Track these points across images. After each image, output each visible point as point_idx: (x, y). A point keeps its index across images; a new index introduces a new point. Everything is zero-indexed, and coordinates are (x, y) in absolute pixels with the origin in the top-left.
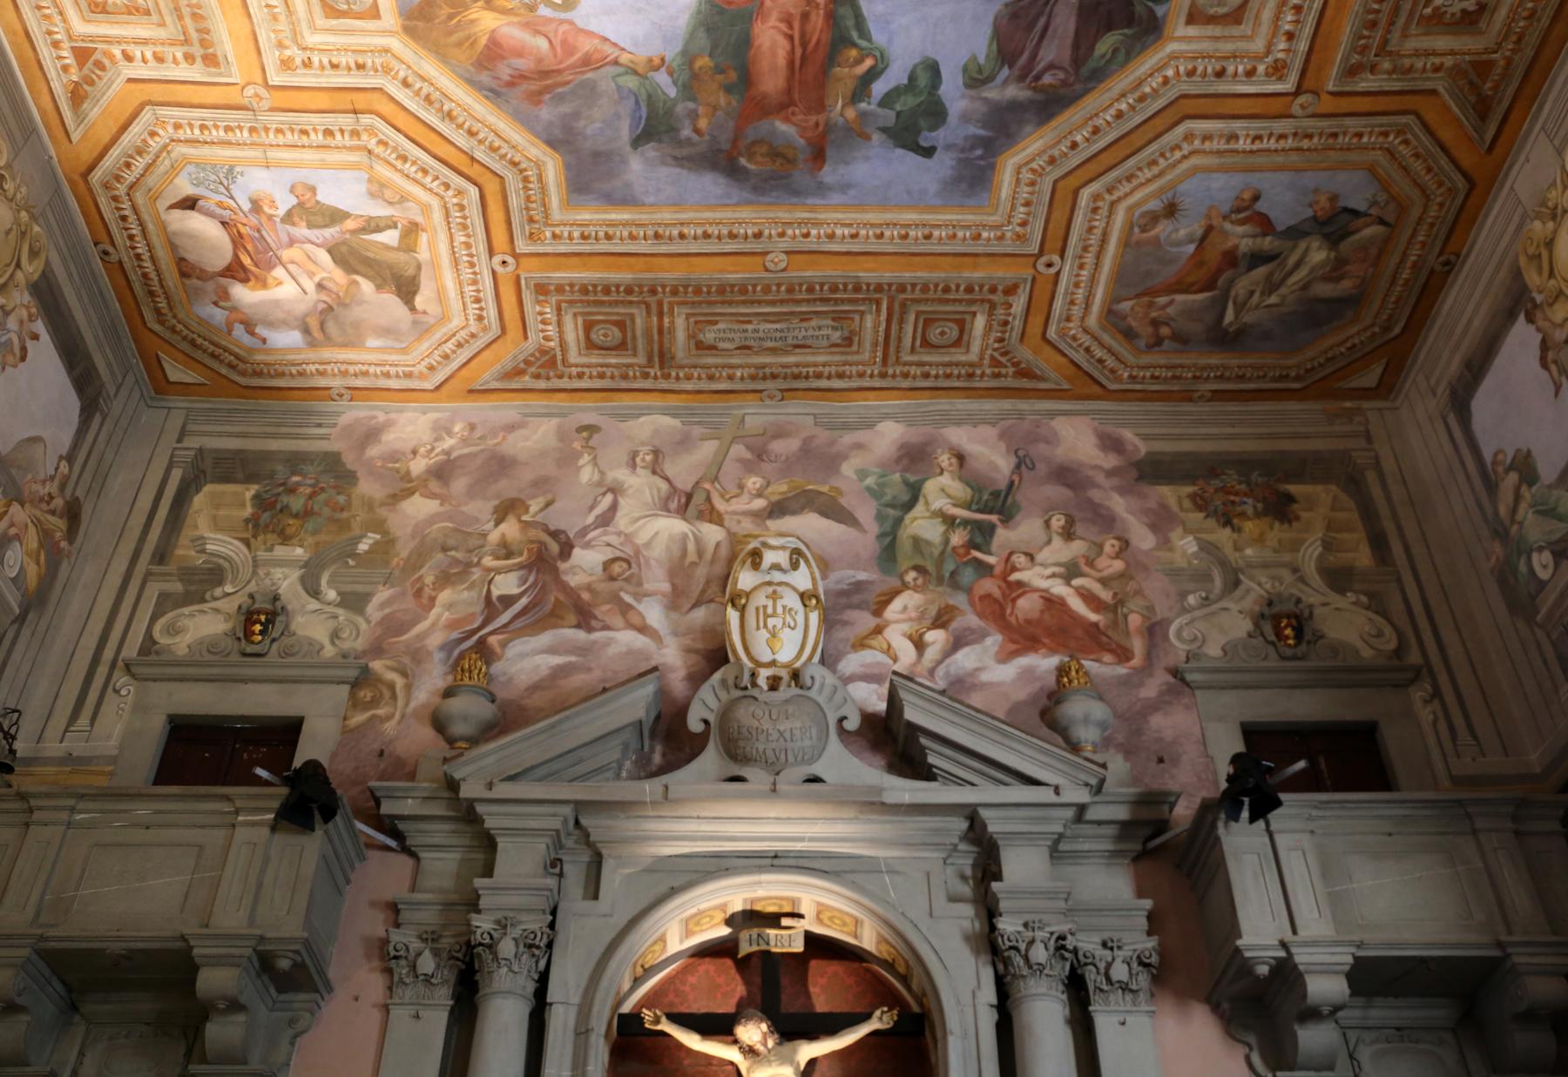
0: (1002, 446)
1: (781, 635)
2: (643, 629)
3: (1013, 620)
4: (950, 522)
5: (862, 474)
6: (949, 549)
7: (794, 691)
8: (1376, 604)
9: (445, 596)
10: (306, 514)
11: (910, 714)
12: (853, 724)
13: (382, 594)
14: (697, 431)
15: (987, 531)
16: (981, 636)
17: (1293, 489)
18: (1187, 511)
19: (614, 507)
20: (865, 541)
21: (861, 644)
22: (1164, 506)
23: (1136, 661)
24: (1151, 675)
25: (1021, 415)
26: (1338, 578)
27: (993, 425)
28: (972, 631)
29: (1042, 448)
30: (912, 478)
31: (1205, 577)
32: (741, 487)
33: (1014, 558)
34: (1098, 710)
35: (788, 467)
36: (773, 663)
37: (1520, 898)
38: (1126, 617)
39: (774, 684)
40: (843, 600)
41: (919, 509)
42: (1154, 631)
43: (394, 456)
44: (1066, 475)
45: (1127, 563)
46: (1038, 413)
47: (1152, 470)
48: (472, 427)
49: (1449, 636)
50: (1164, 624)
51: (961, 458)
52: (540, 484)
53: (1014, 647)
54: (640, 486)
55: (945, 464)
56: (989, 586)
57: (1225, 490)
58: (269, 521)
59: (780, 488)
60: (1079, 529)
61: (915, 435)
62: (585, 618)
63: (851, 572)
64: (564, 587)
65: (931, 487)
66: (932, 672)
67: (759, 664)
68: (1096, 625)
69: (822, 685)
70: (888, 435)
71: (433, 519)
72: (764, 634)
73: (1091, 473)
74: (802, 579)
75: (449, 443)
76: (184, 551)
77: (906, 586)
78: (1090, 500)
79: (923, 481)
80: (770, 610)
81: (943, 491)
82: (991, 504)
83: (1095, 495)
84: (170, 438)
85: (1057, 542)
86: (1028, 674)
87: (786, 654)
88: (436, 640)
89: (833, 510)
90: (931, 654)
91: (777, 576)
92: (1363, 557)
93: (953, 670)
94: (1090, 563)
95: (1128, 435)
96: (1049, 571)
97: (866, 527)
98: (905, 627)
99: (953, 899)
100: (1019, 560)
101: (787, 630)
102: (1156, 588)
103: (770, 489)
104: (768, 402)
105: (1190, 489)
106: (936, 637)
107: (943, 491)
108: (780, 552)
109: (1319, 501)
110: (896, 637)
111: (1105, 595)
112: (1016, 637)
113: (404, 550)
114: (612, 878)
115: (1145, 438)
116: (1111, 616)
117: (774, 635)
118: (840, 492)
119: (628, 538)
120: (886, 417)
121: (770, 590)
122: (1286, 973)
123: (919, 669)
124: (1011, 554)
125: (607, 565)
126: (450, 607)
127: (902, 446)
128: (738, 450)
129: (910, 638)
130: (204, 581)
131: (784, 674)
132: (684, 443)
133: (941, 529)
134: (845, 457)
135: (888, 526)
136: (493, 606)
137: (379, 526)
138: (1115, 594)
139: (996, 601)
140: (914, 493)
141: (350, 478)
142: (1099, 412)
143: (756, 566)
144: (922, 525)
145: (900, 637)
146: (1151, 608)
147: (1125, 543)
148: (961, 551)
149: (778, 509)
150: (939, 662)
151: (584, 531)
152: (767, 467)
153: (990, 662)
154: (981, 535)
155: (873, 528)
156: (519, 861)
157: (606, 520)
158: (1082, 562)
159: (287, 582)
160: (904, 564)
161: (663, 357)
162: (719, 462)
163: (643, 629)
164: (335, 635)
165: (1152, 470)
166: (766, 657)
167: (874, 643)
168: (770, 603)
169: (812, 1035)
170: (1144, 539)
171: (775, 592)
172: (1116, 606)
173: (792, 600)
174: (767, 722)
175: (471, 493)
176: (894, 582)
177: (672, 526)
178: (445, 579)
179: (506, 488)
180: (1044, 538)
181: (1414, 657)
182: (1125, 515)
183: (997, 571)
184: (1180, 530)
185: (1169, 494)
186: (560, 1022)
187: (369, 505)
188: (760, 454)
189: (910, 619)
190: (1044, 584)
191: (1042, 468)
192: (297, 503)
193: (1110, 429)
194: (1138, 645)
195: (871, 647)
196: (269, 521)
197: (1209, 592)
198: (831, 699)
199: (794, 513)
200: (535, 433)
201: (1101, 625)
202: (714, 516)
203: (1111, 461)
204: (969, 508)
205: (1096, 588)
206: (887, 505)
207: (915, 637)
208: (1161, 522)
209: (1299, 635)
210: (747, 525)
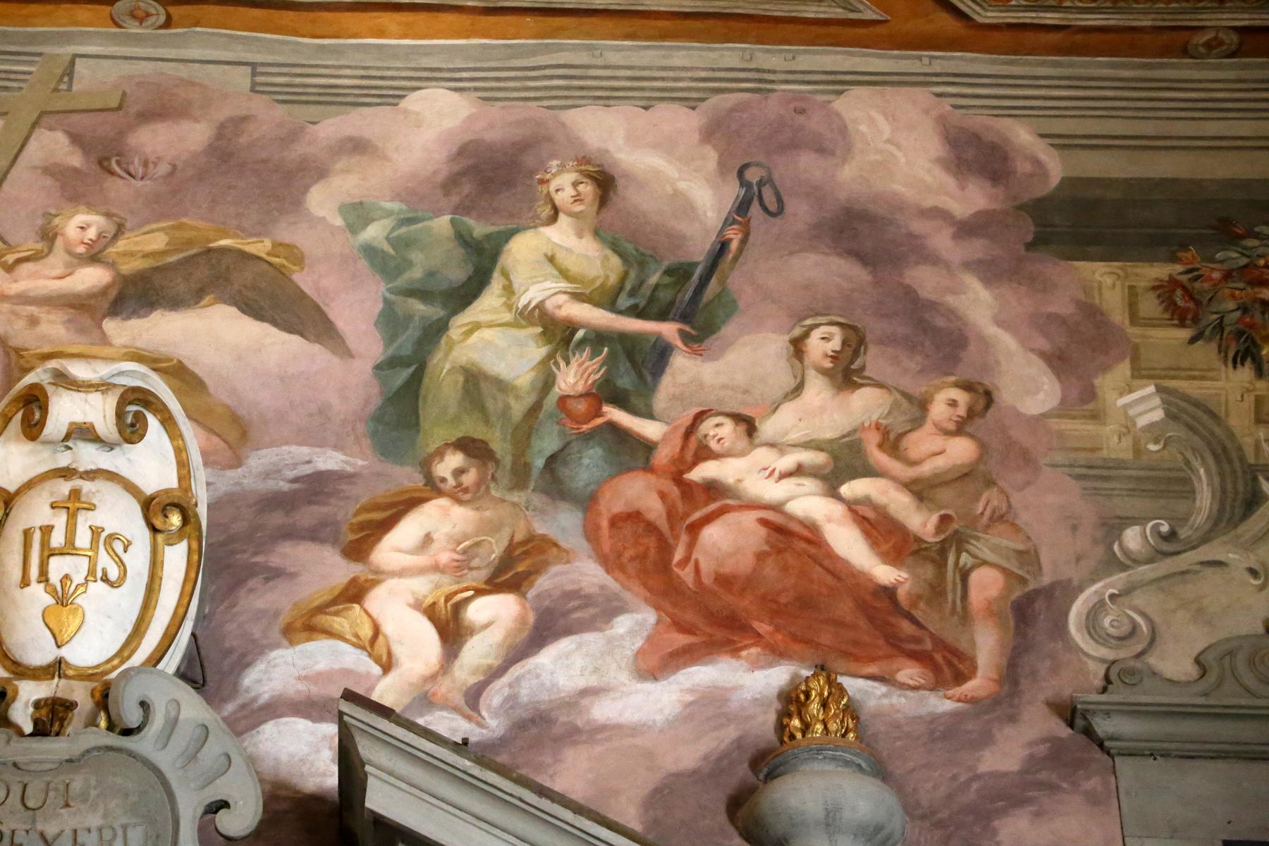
0: (711, 157)
3: (687, 575)
5: (358, 214)
6: (551, 401)
7: (101, 736)
11: (381, 799)
15: (647, 361)
16: (609, 610)
18: (1151, 323)
20: (345, 378)
21: (307, 626)
22: (1092, 312)
23: (976, 685)
24: (1012, 719)
25: (762, 82)
27: (692, 104)
28: (587, 600)
29: (807, 165)
30: (479, 229)
31: (1181, 486)
32: (49, 236)
33: (707, 427)
34: (862, 798)
35: (176, 188)
36: (57, 668)
38: (965, 575)
39: (52, 717)
40: (277, 519)
41: (489, 303)
44: (860, 231)
45: (983, 447)
46: (803, 77)
47: (1070, 224)
53: (682, 640)
55: (564, 197)
56: (639, 492)
59: (147, 243)
60: (874, 361)
61: (498, 123)
63: (303, 451)
65: (523, 250)
66: (474, 696)
67: (22, 671)
68: (888, 593)
69: (173, 723)
70: (434, 121)
72: (38, 597)
73: (918, 226)
74: (151, 463)
77: (433, 488)
78: (910, 294)
79: (509, 235)
80: (57, 539)
81: (552, 260)
82: (665, 296)
83: (924, 280)
85: (817, 391)
86: (709, 706)
87: (91, 647)
89: (279, 301)
90: (477, 653)
91: (88, 456)
93: (524, 693)
94: (892, 443)
95: (1022, 135)
96: (788, 461)
97: (352, 342)
98: (422, 586)
100: (721, 431)
101: (98, 587)
102: (1047, 511)
103: (122, 245)
104: (134, 29)
105: (1159, 271)
106: (494, 614)
107: (552, 260)
108: (95, 398)
110: (398, 611)
111: (921, 522)
112: (690, 616)
115: (1063, 143)
116: (928, 572)
117: (63, 600)
118: (298, 258)
120: (432, 77)
121: (64, 487)
123: (443, 688)
124: (700, 417)
127: (462, 152)
129: (431, 613)
131: (81, 694)
133: (538, 352)
134: (322, 173)
135: (406, 342)
138: (945, 519)
139: (651, 528)
140: (482, 264)
142: (957, 77)
143: (33, 430)
144: (493, 343)
146: (1029, 557)
147: (984, 398)
148: (581, 407)
149: (138, 293)
150: (495, 673)
152: (119, 189)
153: (624, 677)
154: (633, 369)
155: (368, 345)
158: (871, 441)
160: (435, 433)
165: (1070, 224)
166: (39, 652)
167: (338, 623)
168: (60, 521)
170: (1029, 388)
171: (75, 494)
172: (943, 549)
173: (118, 515)
176: (407, 477)
180: (789, 382)
182: (992, 330)
183: (663, 456)
184: (1123, 370)
185: (1105, 281)
188: (107, 157)
189: (436, 568)
190: (772, 491)
191: (800, 212)
193: (979, 121)
194: (986, 646)
195: (330, 634)
197: (1177, 521)
198: (192, 757)
199: (176, 304)
201: (902, 593)
203: (972, 198)
204: (612, 306)
205: (900, 504)
206: (411, 292)
207: (444, 610)
208: (1078, 350)
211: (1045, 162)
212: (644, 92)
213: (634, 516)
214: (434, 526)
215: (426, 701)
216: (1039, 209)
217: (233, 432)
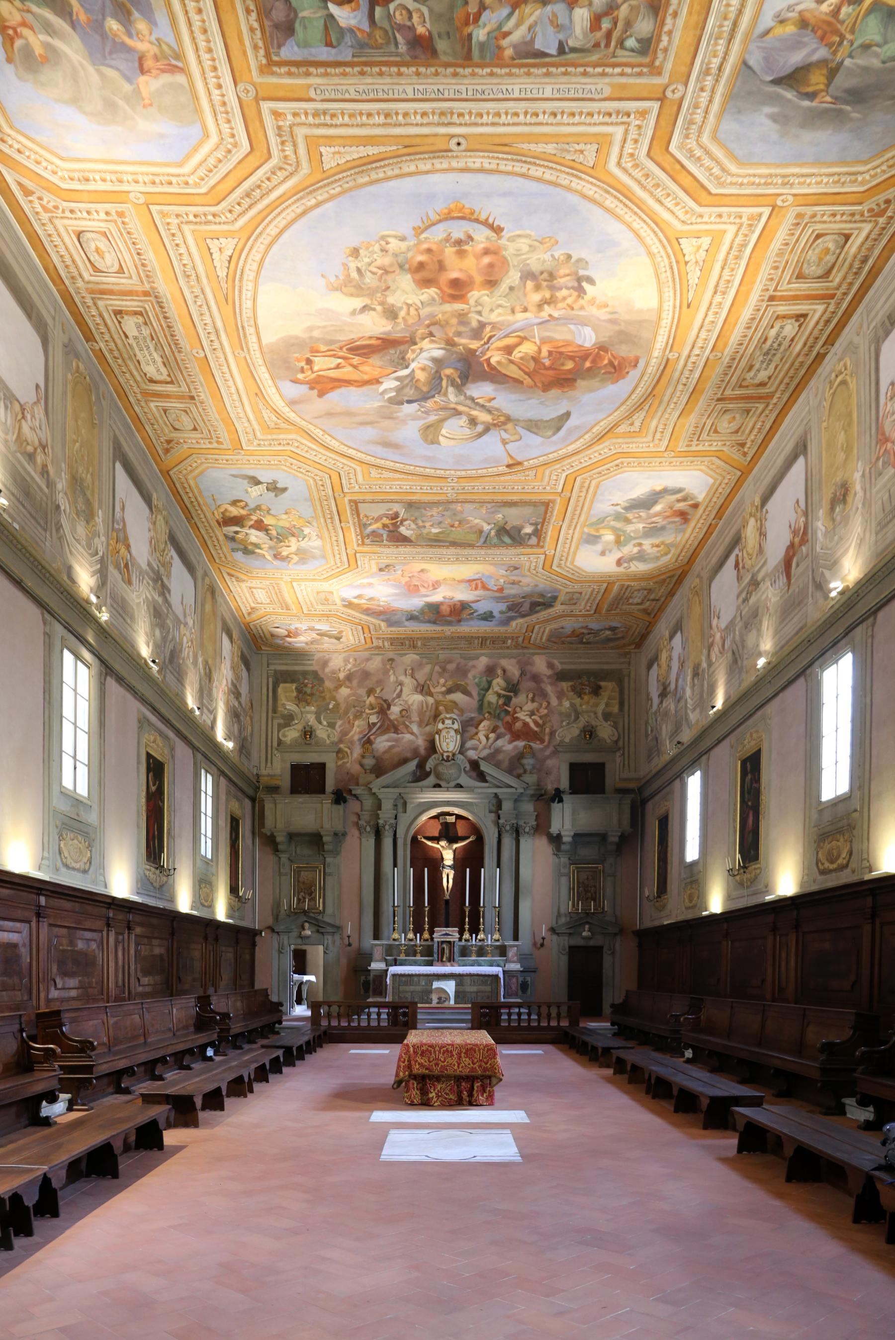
1: (449, 743)
2: (412, 733)
4: (499, 695)
5: (474, 677)
8: (615, 726)
9: (357, 723)
10: (312, 695)
12: (468, 769)
13: (339, 723)
14: (425, 660)
17: (602, 684)
19: (401, 691)
20: (474, 703)
21: (472, 738)
26: (607, 716)
31: (570, 715)
37: (615, 819)
41: (490, 691)
42: (552, 734)
43: (334, 672)
44: (536, 678)
47: (561, 676)
48: (355, 660)
49: (632, 736)
50: (555, 731)
51: (504, 671)
52: (379, 682)
54: (408, 682)
56: (508, 719)
57: (582, 684)
58: (302, 697)
59: (450, 683)
60: (536, 698)
62: (396, 731)
64: (389, 719)
65: (495, 682)
71: (349, 696)
75: (349, 666)
76: (280, 709)
81: (498, 683)
83: (543, 685)
84: (265, 665)
88: (356, 738)
89: (466, 692)
90: (491, 741)
92: (616, 709)
95: (556, 662)
99: (490, 812)
100: (518, 709)
105: (570, 683)
106: (492, 736)
109: (609, 687)
111: (540, 722)
113: (343, 706)
114: (409, 807)
115: (562, 663)
119: (406, 702)
122: (559, 836)
125: (401, 712)
126: (359, 726)
128: (437, 668)
130: (289, 719)
132: (421, 665)
136: (371, 726)
137: (334, 698)
140: (490, 684)
141: (321, 681)
144: (491, 697)
145: (482, 741)
147: (549, 703)
149: (450, 691)
151: (394, 700)
152: (446, 675)
154: (508, 700)
156: (387, 805)
157: (399, 696)
159: (312, 719)
160: (485, 711)
161: (414, 647)
162: (431, 674)
163: (412, 733)
164: (329, 736)
165: (561, 676)
169: (456, 842)
170: (554, 702)
173: (453, 733)
174: (447, 770)
175: (360, 685)
177: (418, 698)
178: (356, 717)
179: (369, 683)
181: (620, 744)
185: (565, 685)
186: (400, 842)
187: (330, 691)
188: (444, 669)
190: (523, 718)
191: (528, 675)
192: (308, 690)
194: (547, 738)
196: (302, 697)
200: (375, 664)
202: (431, 694)
203: (549, 672)
208: (560, 696)
209: (591, 736)
210: (440, 697)
211: (559, 667)
212: (510, 657)
213: (507, 722)
214: (485, 724)
215: (485, 748)
216: (557, 674)
217: (462, 711)
